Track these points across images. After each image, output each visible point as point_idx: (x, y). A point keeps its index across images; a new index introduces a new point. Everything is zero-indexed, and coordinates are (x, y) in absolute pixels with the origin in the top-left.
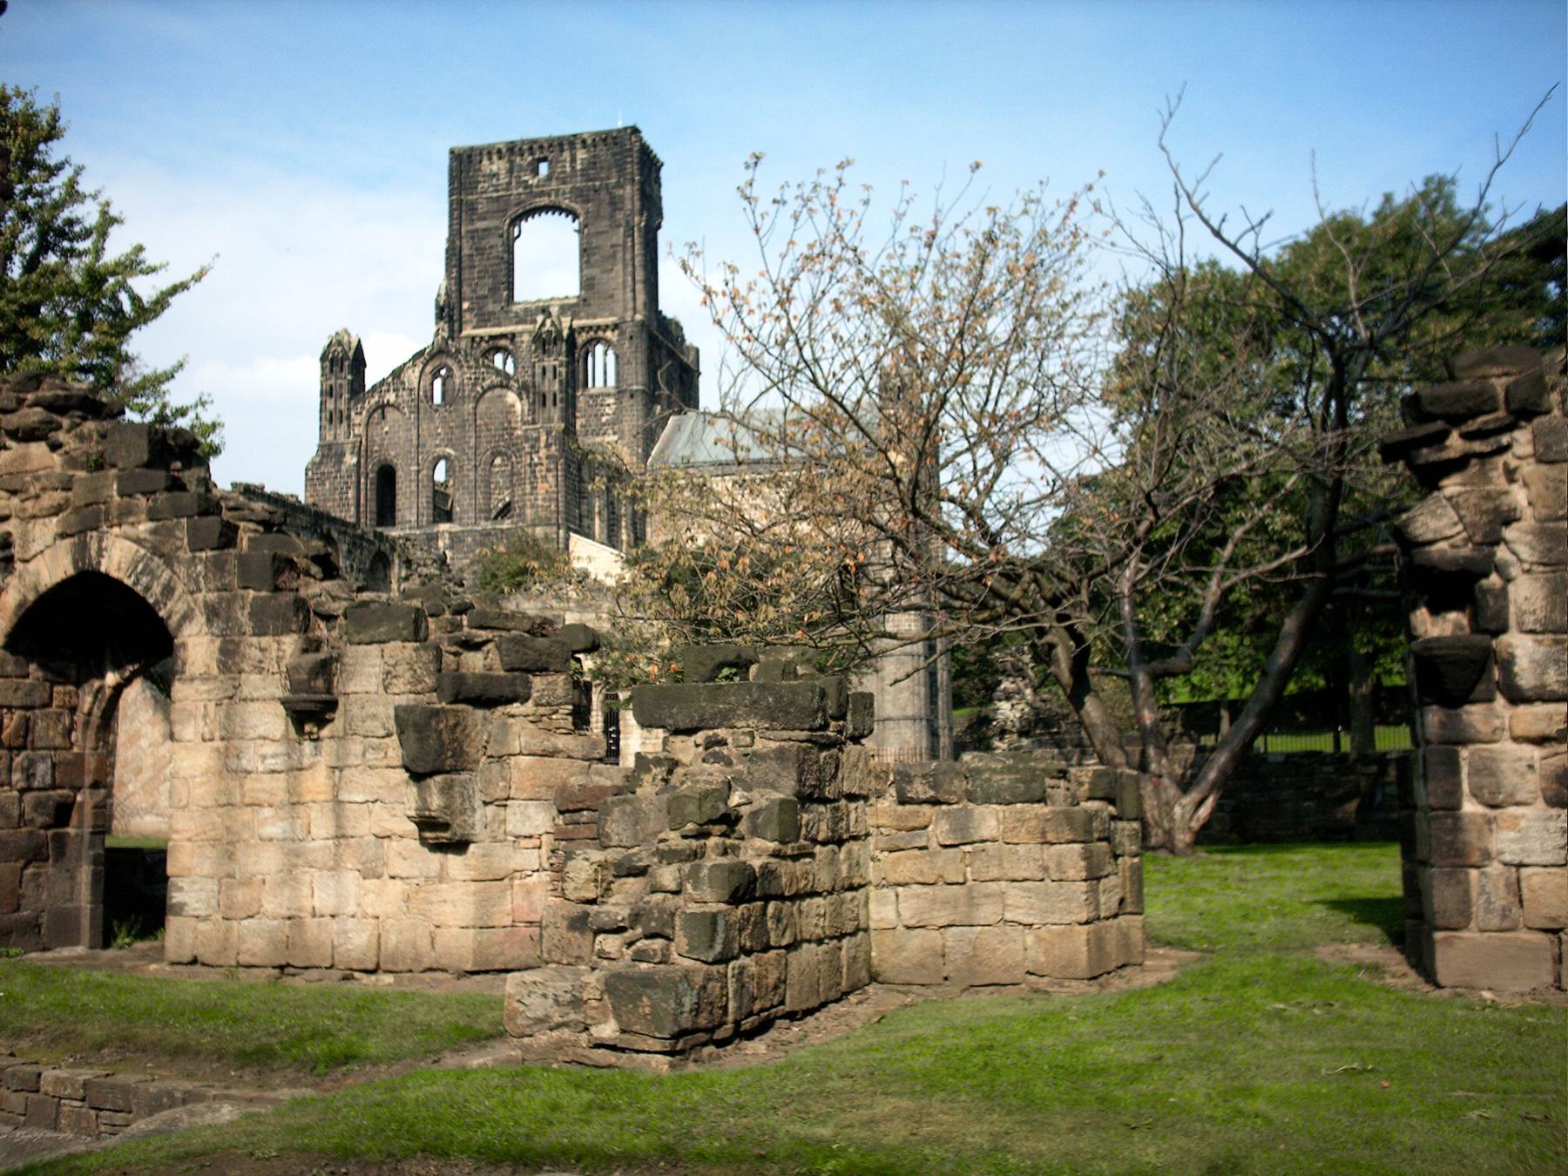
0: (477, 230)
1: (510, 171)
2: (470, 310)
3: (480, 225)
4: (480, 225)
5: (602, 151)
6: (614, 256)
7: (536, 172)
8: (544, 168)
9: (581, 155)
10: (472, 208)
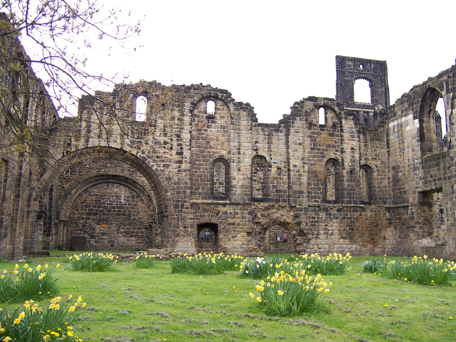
1: (354, 66)
3: (346, 78)
4: (346, 78)
5: (378, 65)
6: (382, 94)
10: (343, 73)
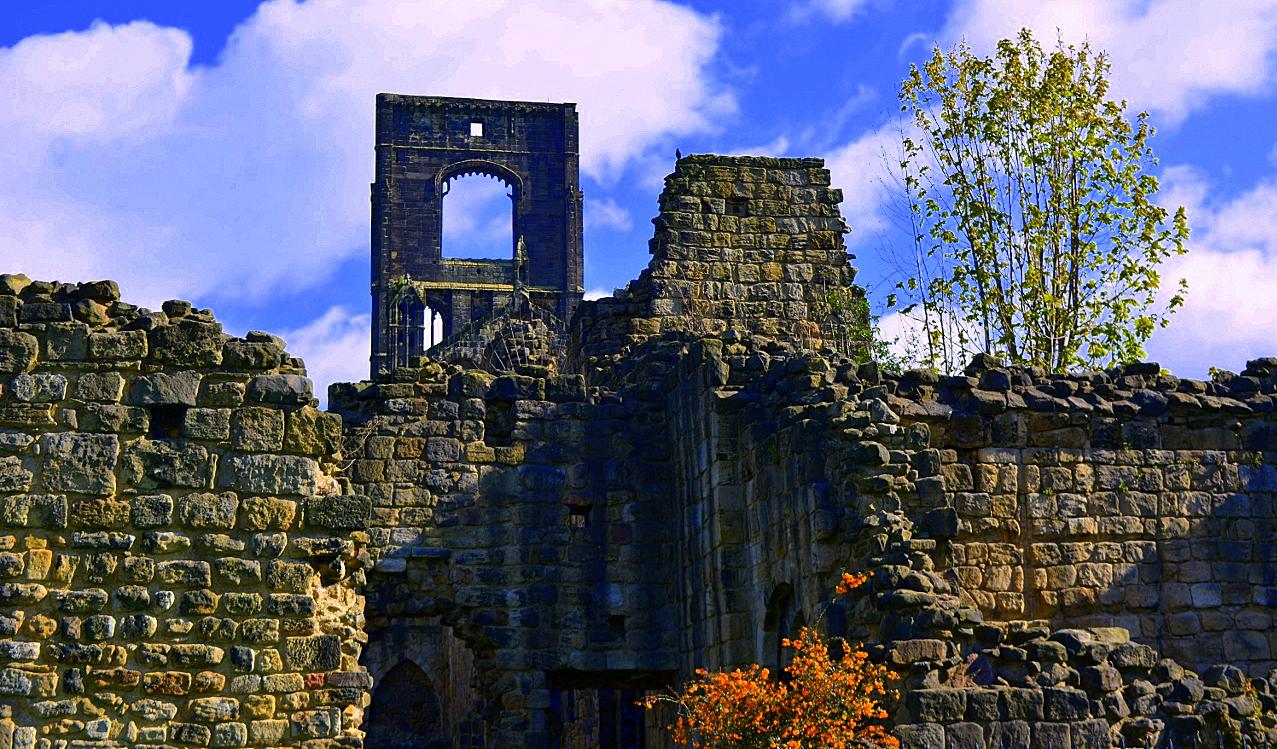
0: (406, 181)
2: (399, 260)
3: (411, 175)
4: (411, 175)
7: (468, 131)
8: (476, 130)
9: (519, 122)
